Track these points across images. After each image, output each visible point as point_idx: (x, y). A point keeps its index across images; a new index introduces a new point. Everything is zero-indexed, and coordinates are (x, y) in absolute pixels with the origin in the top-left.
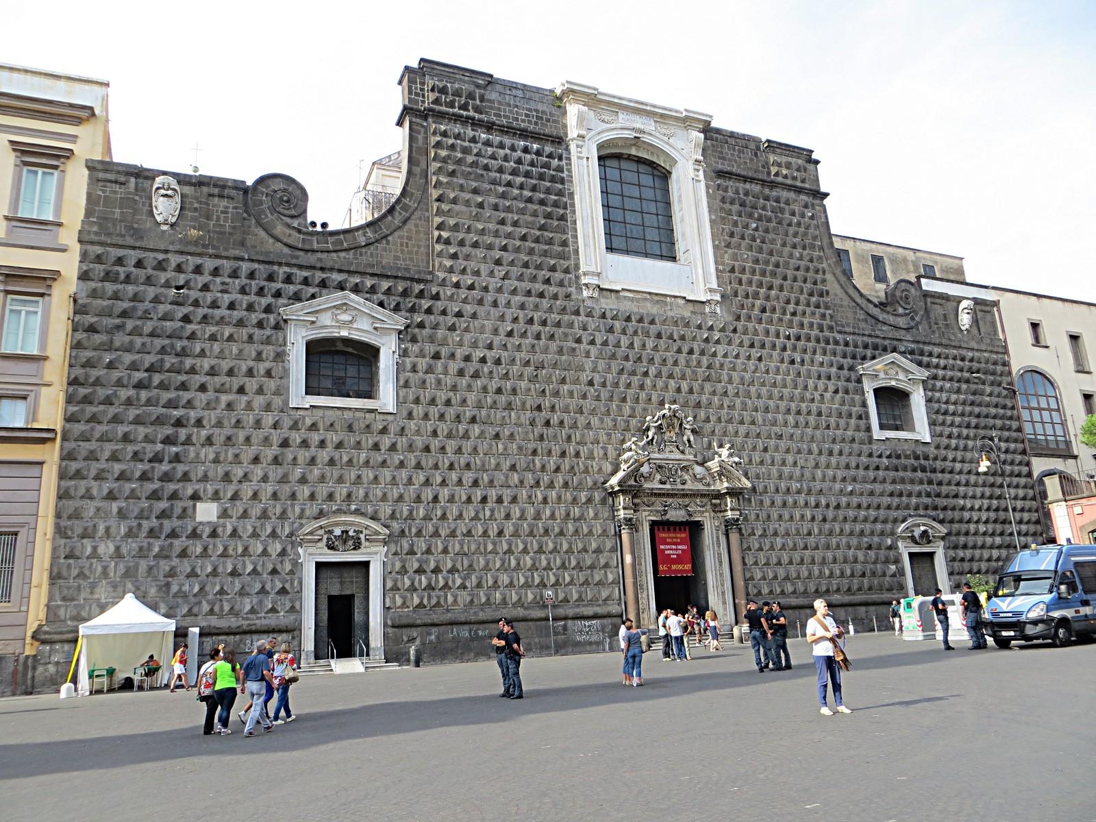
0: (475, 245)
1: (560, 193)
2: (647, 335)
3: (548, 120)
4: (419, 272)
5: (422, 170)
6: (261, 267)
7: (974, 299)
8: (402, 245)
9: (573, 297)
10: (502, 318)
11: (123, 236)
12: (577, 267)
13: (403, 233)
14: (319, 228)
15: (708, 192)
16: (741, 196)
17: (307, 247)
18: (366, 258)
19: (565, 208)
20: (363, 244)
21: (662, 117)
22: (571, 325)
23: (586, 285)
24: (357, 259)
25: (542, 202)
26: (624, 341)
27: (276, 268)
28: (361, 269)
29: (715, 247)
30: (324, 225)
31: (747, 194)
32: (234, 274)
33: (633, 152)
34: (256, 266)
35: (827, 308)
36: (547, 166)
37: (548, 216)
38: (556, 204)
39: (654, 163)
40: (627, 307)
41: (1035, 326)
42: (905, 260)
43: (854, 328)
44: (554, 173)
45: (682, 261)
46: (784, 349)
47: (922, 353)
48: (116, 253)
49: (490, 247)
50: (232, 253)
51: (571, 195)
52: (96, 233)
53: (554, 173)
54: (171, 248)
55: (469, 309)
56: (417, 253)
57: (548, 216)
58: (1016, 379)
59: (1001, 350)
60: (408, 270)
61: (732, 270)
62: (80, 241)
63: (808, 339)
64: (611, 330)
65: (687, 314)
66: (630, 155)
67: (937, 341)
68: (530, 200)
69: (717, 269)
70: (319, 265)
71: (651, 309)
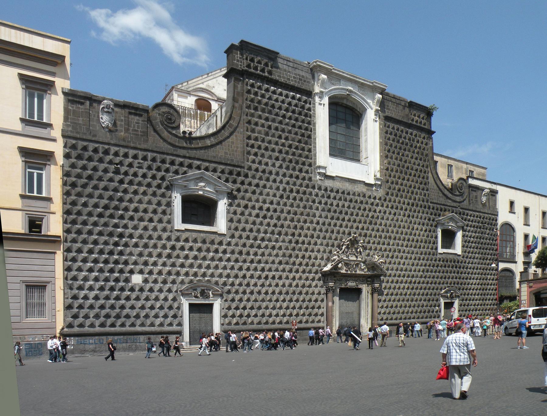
0: (266, 149)
1: (309, 123)
2: (345, 200)
3: (305, 81)
4: (238, 162)
6: (158, 155)
8: (229, 146)
9: (313, 179)
10: (278, 189)
11: (85, 134)
12: (315, 163)
13: (230, 140)
14: (187, 135)
15: (380, 127)
16: (395, 130)
17: (180, 145)
18: (211, 154)
19: (311, 131)
20: (209, 144)
21: (362, 86)
22: (311, 194)
23: (319, 173)
24: (206, 153)
25: (300, 127)
26: (335, 203)
27: (165, 156)
28: (210, 159)
29: (381, 156)
30: (190, 133)
31: (398, 130)
32: (145, 158)
33: (345, 102)
34: (155, 154)
35: (427, 190)
36: (303, 107)
37: (303, 135)
38: (306, 129)
39: (354, 108)
40: (337, 185)
41: (512, 203)
43: (437, 200)
44: (307, 111)
45: (363, 163)
46: (406, 210)
47: (464, 214)
48: (81, 144)
49: (273, 150)
50: (143, 146)
51: (314, 124)
52: (71, 131)
53: (307, 111)
54: (112, 142)
55: (262, 183)
56: (236, 151)
57: (303, 135)
58: (499, 227)
59: (496, 214)
60: (232, 160)
61: (387, 169)
62: (64, 136)
63: (417, 206)
64: (329, 197)
66: (342, 103)
67: (471, 208)
68: (294, 126)
69: (380, 168)
70: (187, 155)
71: (348, 187)
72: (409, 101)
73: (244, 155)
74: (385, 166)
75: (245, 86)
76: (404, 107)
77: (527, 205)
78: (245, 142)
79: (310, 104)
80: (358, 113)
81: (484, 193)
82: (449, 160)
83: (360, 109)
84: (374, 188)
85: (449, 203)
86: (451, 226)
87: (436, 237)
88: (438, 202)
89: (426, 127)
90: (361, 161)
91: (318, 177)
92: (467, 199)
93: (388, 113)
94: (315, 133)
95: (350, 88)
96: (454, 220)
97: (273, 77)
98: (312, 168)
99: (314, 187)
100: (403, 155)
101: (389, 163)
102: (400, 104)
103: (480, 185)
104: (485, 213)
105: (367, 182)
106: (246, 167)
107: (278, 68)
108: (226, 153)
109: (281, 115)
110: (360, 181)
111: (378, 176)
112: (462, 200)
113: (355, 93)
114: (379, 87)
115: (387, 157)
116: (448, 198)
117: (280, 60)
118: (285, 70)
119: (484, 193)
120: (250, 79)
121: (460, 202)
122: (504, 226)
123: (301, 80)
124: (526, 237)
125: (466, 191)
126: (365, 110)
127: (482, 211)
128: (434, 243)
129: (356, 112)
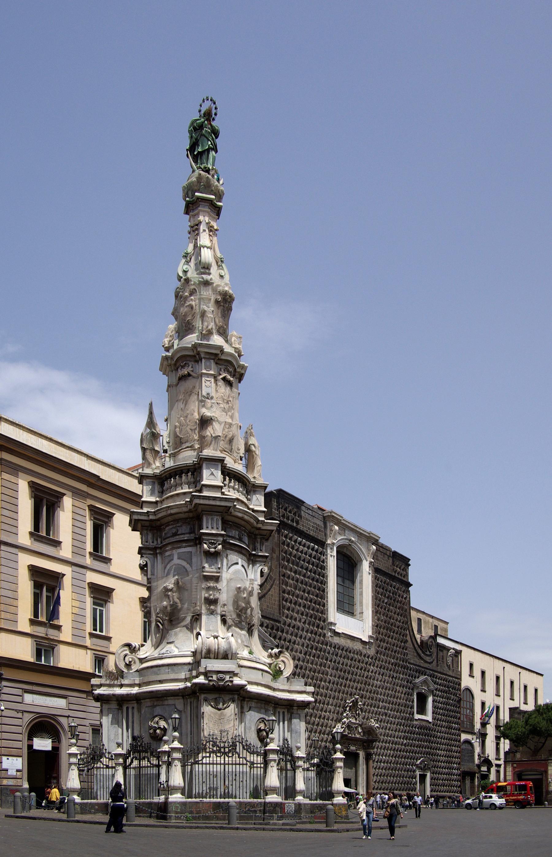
5: (277, 556)
7: (454, 649)
9: (326, 635)
12: (327, 617)
23: (331, 629)
29: (373, 611)
41: (471, 665)
42: (428, 622)
46: (390, 671)
51: (327, 576)
59: (459, 677)
61: (377, 626)
65: (361, 648)
67: (439, 670)
71: (348, 644)
72: (393, 550)
73: (280, 609)
74: (376, 622)
75: (281, 536)
76: (389, 556)
77: (484, 668)
78: (281, 596)
79: (324, 556)
80: (353, 562)
81: (449, 654)
82: (419, 614)
83: (355, 558)
84: (368, 647)
85: (422, 663)
86: (424, 689)
87: (413, 702)
88: (415, 663)
89: (404, 579)
90: (354, 614)
91: (329, 634)
92: (436, 659)
93: (376, 565)
94: (327, 587)
95: (353, 539)
96: (426, 682)
97: (299, 527)
98: (325, 624)
99: (326, 645)
100: (388, 611)
101: (378, 620)
102: (386, 554)
103: (447, 645)
104: (450, 676)
105: (363, 639)
106: (282, 623)
107: (300, 516)
108: (268, 606)
109: (304, 567)
110: (358, 638)
111: (370, 634)
112: (432, 660)
113: (355, 544)
114: (374, 538)
115: (377, 612)
116: (421, 658)
117: (303, 508)
118: (307, 519)
119: (449, 654)
120: (284, 530)
121: (430, 663)
122: (465, 692)
123: (317, 529)
124: (483, 704)
125: (434, 650)
126: (361, 561)
127: (448, 674)
128: (411, 708)
129: (352, 561)
